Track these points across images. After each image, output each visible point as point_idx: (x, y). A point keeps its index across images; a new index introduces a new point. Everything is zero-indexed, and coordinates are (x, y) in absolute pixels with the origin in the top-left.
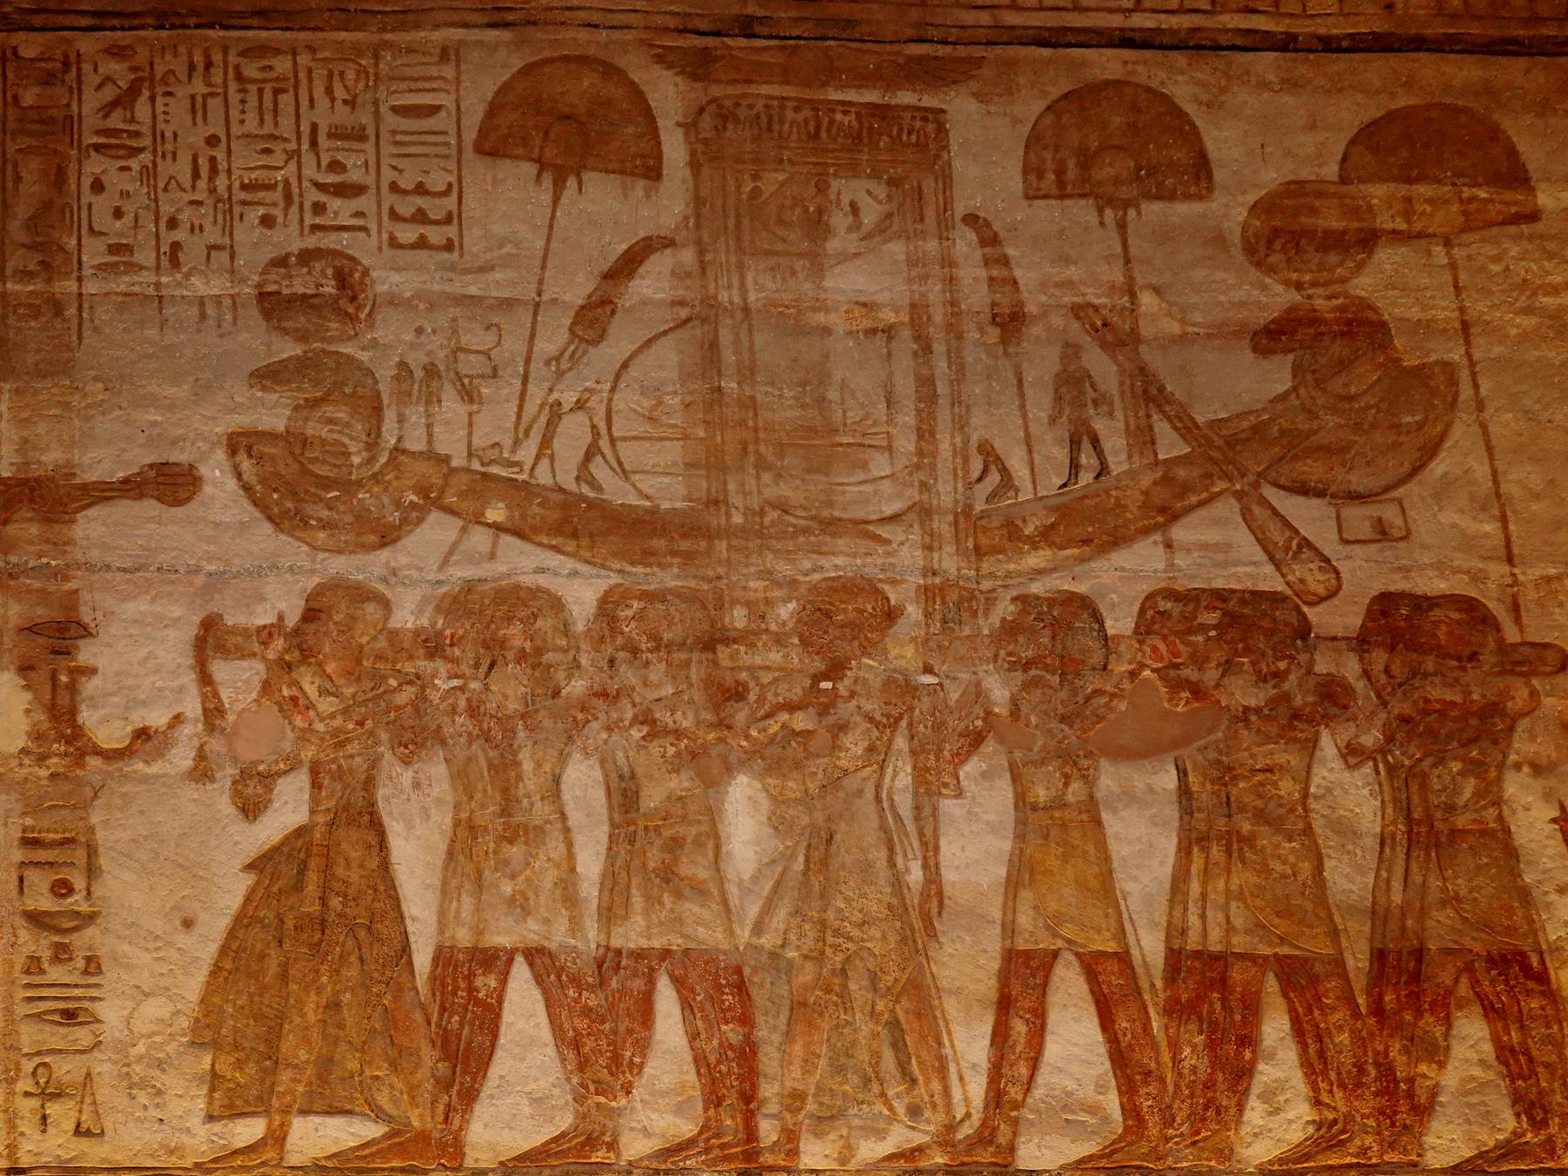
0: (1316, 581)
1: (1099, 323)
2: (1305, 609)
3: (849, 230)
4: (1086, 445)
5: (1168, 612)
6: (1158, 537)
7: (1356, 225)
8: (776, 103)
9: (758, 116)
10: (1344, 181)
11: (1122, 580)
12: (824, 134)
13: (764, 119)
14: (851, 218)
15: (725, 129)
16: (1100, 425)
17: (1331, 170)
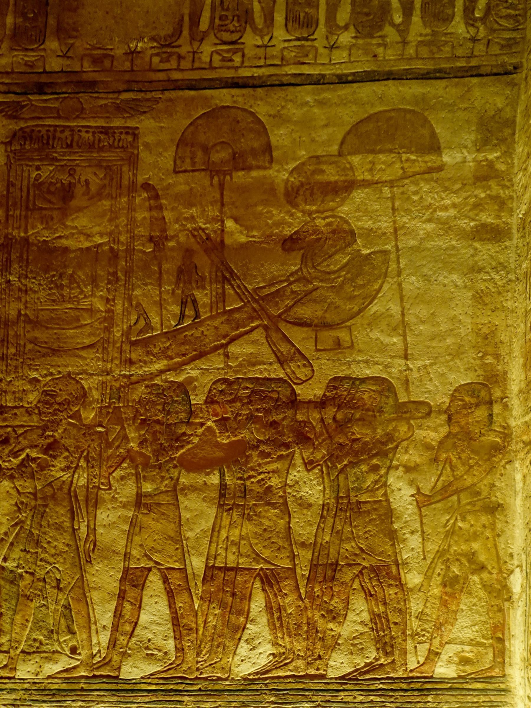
0: (302, 373)
1: (205, 238)
2: (294, 386)
3: (83, 194)
4: (190, 304)
5: (225, 390)
6: (221, 351)
7: (343, 178)
8: (52, 129)
9: (42, 136)
10: (340, 154)
11: (201, 375)
12: (74, 144)
13: (45, 137)
14: (85, 187)
15: (25, 144)
16: (198, 294)
17: (334, 149)
